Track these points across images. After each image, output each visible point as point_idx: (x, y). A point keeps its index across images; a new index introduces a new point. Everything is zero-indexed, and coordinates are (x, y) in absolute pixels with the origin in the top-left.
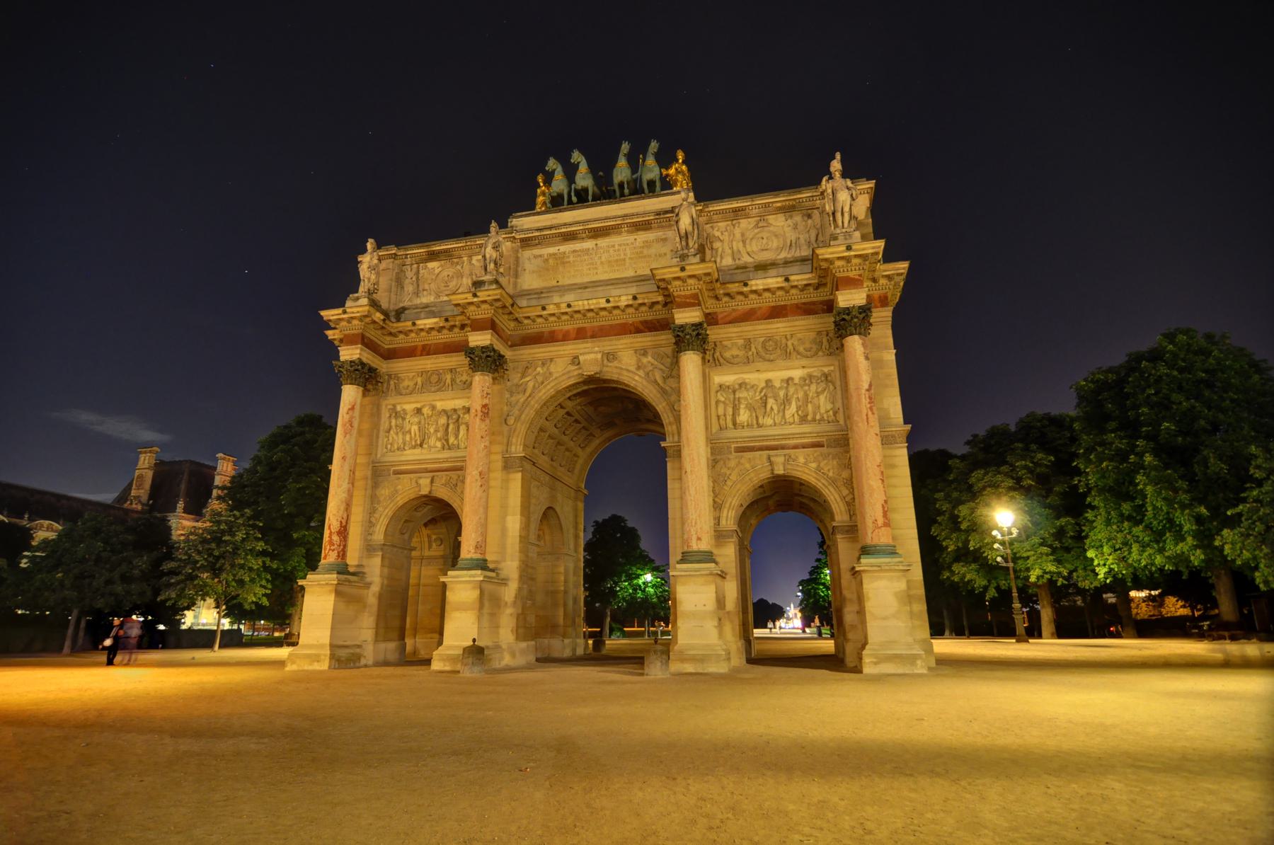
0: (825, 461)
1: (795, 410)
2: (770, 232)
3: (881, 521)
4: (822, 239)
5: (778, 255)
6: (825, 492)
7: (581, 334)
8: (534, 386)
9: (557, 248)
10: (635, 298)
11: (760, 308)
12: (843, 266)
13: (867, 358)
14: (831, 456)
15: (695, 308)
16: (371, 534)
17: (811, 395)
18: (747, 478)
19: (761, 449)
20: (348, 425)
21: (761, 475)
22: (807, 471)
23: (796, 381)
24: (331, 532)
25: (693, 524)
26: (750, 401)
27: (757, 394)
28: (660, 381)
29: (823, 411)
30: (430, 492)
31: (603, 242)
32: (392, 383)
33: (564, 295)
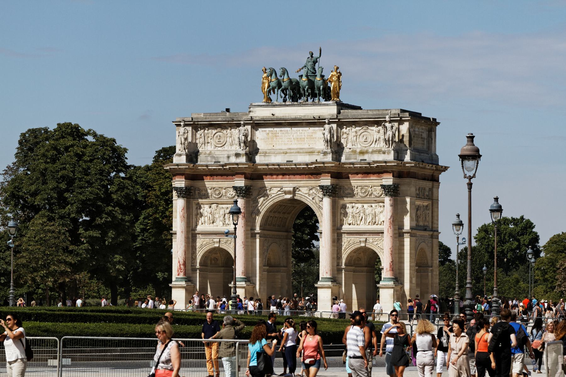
5: (371, 145)
8: (264, 200)
13: (391, 206)
24: (180, 265)
28: (318, 202)
32: (197, 192)
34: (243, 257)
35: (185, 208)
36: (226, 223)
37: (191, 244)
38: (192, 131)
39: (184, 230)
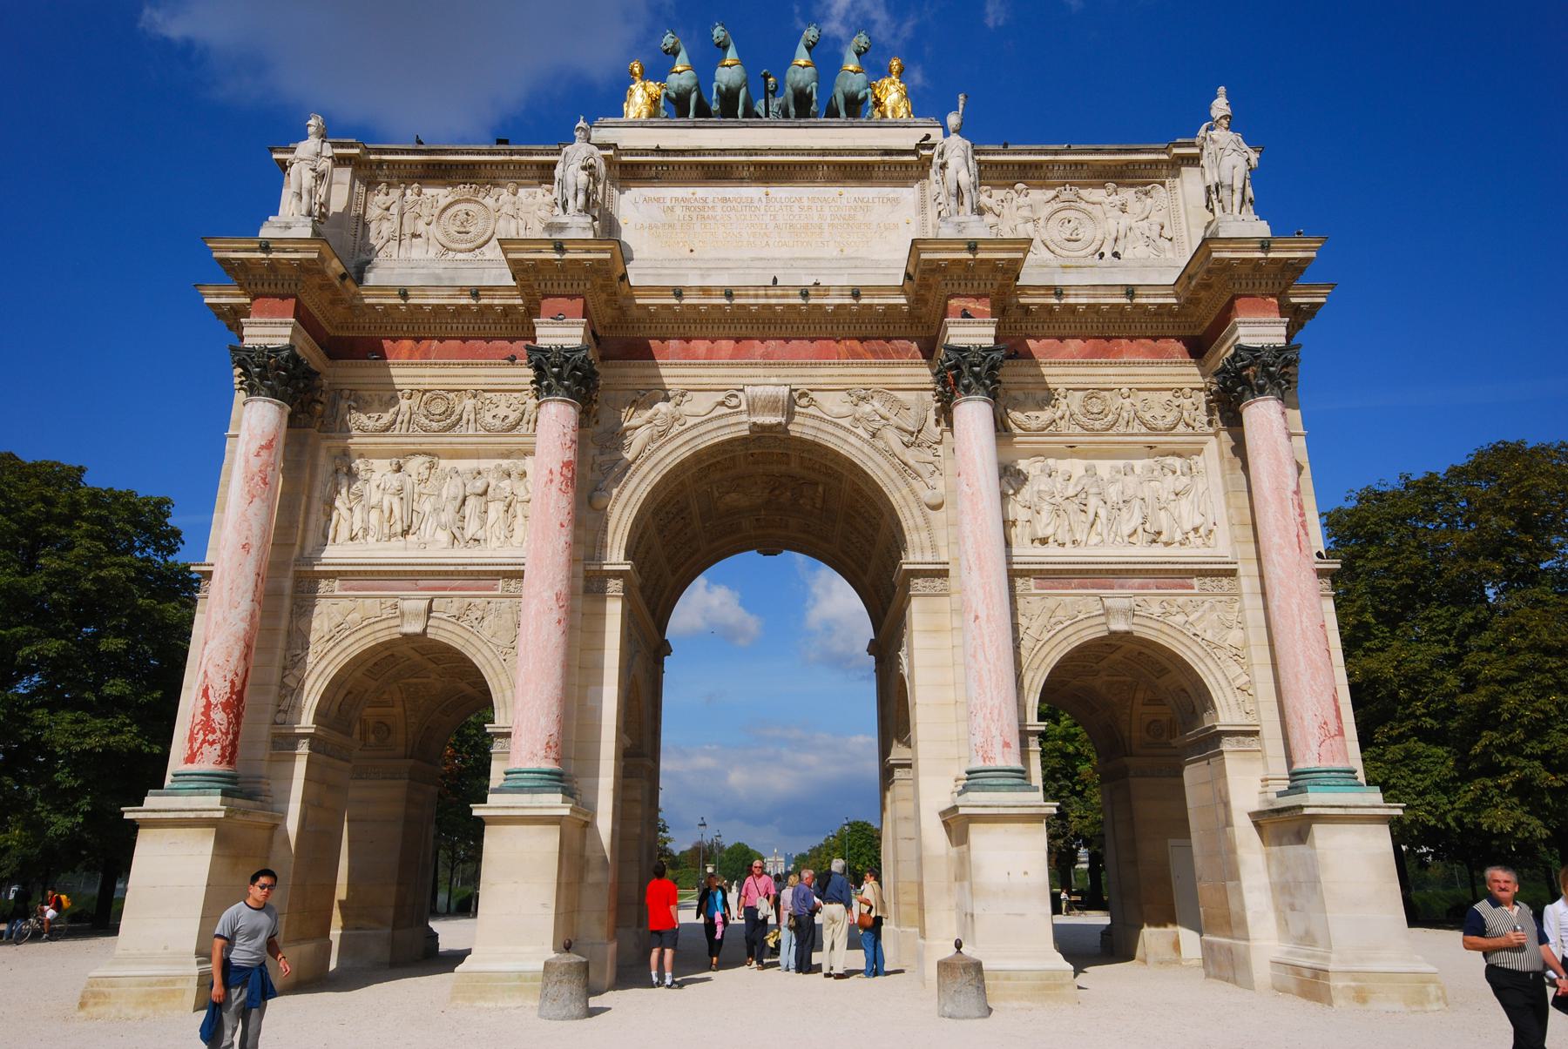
0: (1197, 615)
1: (1141, 521)
2: (1083, 211)
3: (1333, 728)
4: (1167, 233)
6: (1200, 668)
9: (691, 190)
12: (1247, 275)
14: (1207, 605)
15: (986, 320)
16: (286, 712)
17: (1165, 496)
18: (1060, 636)
20: (257, 478)
21: (1084, 633)
22: (1166, 629)
23: (1138, 470)
24: (208, 706)
25: (996, 717)
26: (1060, 500)
28: (898, 448)
29: (1188, 527)
30: (425, 630)
33: (709, 275)
34: (557, 671)
35: (279, 445)
36: (467, 538)
37: (284, 624)
38: (352, 187)
39: (255, 542)
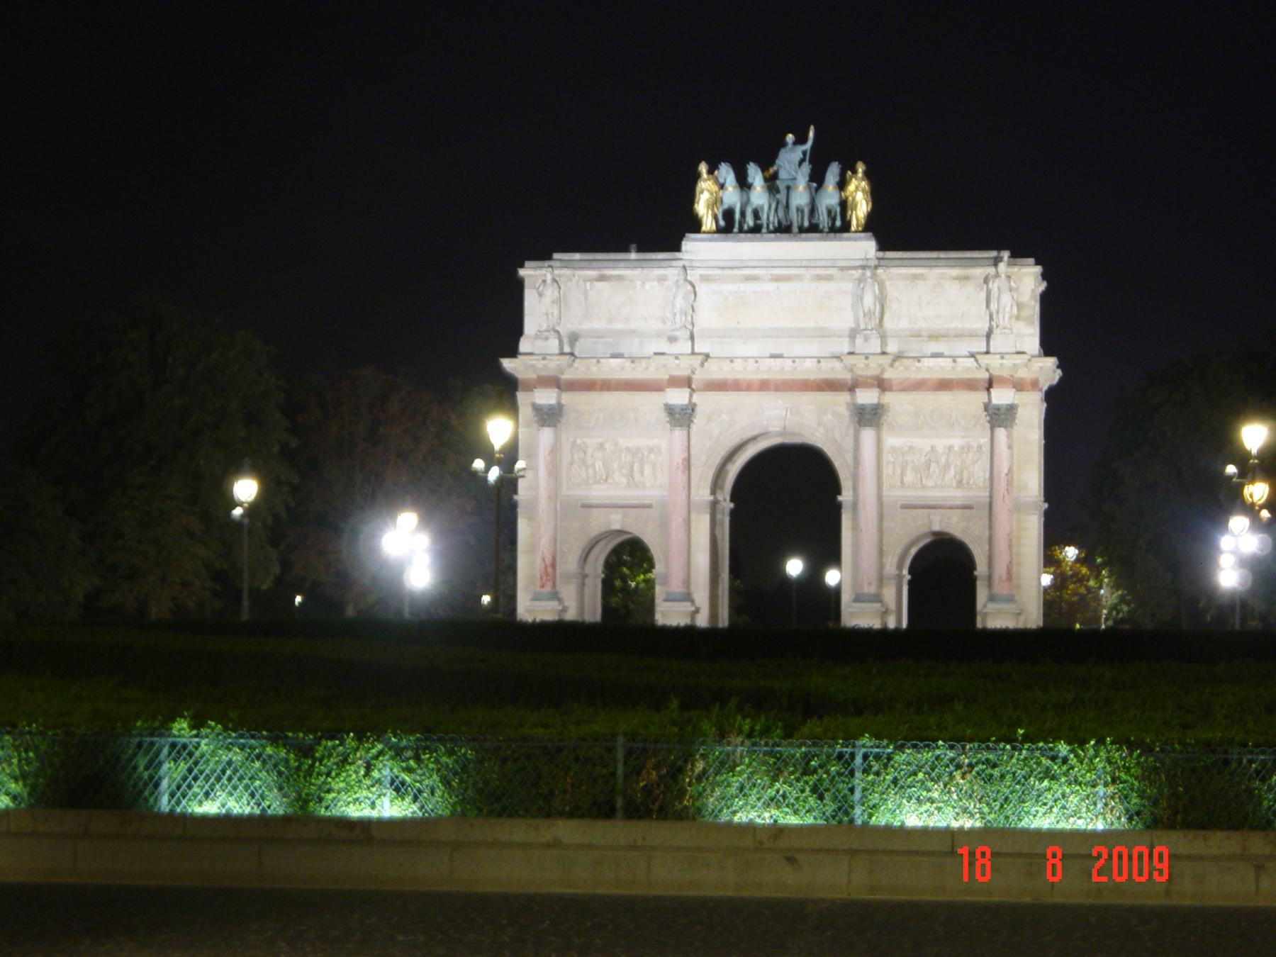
3: (1004, 577)
7: (764, 386)
10: (819, 362)
11: (930, 379)
19: (923, 507)
23: (956, 448)
27: (923, 457)
31: (784, 286)
